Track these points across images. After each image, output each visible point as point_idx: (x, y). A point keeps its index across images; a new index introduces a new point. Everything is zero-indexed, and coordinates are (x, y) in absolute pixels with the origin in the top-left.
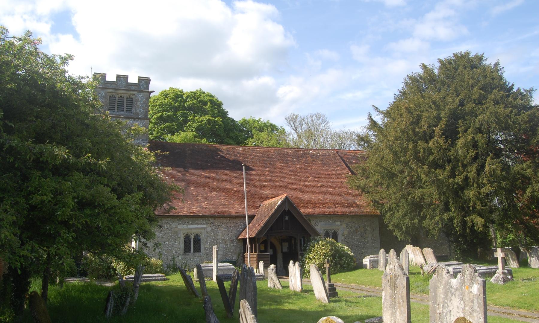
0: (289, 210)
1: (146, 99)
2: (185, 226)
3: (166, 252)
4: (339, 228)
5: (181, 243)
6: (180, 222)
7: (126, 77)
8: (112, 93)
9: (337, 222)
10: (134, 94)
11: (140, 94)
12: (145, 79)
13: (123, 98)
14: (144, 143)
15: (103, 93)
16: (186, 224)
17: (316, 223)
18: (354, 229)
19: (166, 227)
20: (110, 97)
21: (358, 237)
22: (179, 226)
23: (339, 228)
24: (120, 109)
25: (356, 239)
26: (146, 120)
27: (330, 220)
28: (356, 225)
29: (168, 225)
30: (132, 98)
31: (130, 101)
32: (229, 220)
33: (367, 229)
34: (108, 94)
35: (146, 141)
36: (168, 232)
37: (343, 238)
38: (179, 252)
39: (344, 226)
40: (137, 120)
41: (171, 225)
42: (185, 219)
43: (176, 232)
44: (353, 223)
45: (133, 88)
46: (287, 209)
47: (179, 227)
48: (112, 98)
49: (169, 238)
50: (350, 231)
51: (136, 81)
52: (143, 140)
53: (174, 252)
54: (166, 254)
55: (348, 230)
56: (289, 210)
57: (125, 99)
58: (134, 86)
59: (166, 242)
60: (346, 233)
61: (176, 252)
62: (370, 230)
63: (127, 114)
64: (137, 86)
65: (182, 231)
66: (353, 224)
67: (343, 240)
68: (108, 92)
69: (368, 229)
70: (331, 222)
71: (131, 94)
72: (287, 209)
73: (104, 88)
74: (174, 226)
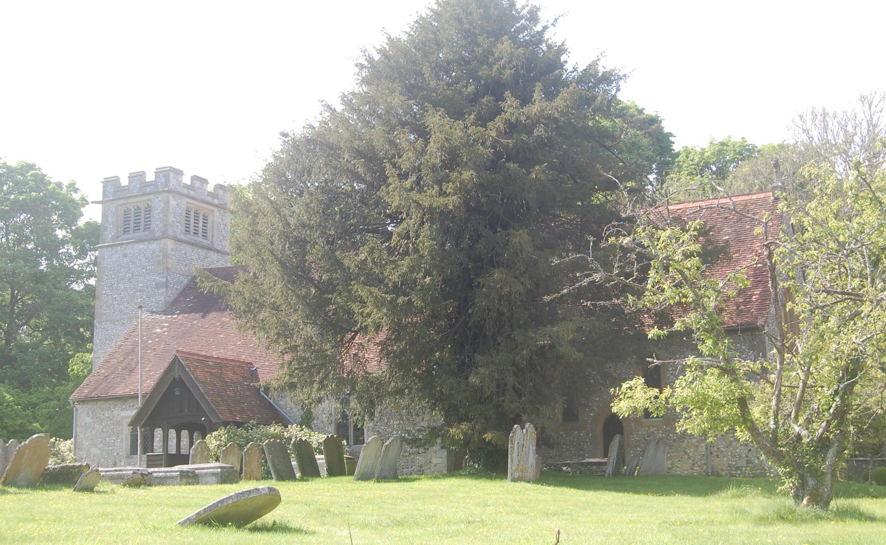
1: (165, 204)
2: (129, 412)
5: (124, 439)
6: (124, 407)
7: (141, 175)
8: (124, 204)
10: (151, 200)
11: (158, 198)
12: (163, 171)
13: (140, 209)
16: (131, 408)
19: (107, 415)
20: (125, 211)
26: (163, 240)
29: (110, 413)
31: (149, 210)
34: (120, 208)
35: (162, 275)
38: (121, 454)
40: (153, 241)
41: (113, 411)
42: (130, 401)
43: (119, 423)
45: (148, 190)
47: (122, 415)
48: (127, 213)
51: (153, 179)
52: (159, 274)
53: (115, 454)
57: (143, 211)
59: (107, 439)
61: (118, 454)
63: (143, 234)
64: (152, 185)
65: (125, 421)
71: (148, 200)
73: (112, 200)
74: (116, 414)
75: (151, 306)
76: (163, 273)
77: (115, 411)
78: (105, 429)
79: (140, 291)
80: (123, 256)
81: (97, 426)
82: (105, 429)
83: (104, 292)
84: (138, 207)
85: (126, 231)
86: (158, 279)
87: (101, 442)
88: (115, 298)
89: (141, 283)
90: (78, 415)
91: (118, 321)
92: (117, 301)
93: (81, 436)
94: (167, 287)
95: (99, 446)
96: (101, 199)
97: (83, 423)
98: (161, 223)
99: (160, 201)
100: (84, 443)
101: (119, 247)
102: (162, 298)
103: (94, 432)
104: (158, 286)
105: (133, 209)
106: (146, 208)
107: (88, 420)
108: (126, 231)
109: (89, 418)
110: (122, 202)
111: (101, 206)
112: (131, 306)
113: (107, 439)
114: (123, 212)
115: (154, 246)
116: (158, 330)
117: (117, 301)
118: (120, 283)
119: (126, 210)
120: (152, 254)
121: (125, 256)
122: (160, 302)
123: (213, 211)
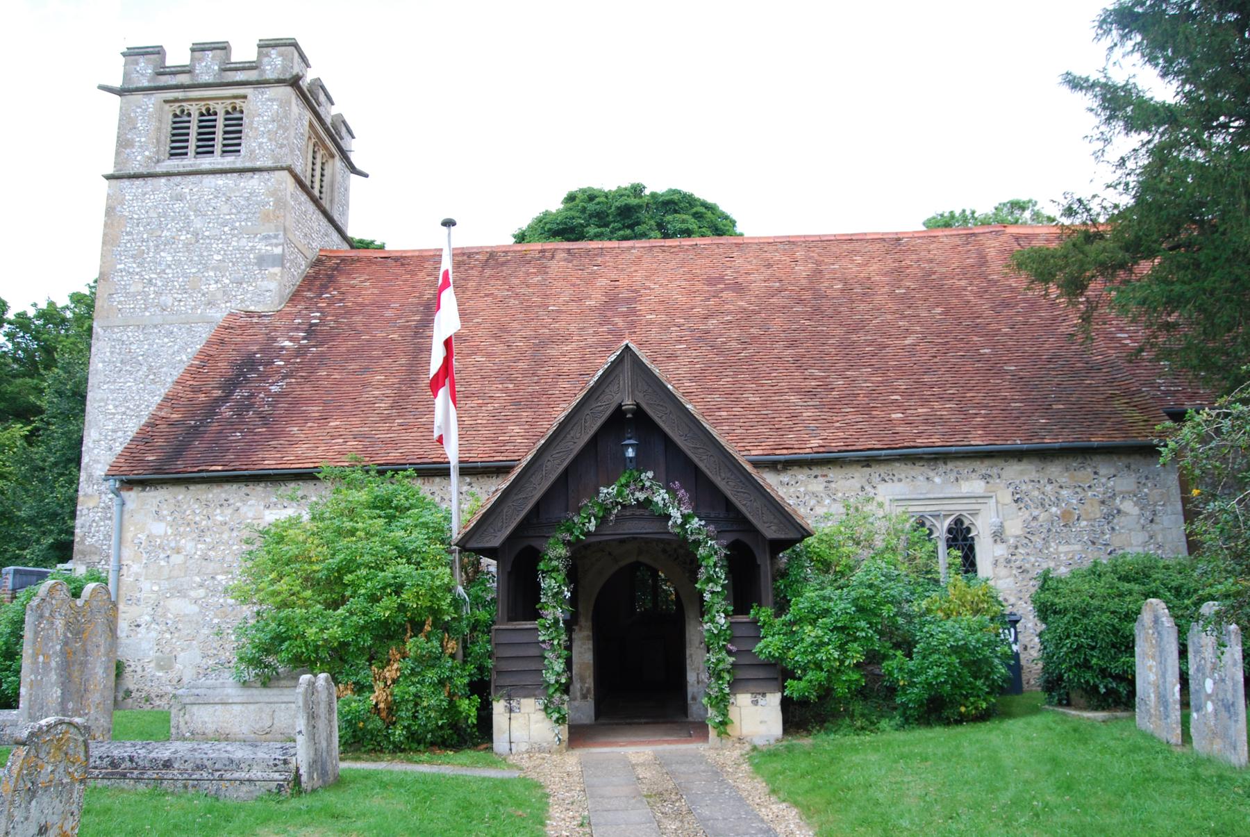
0: (638, 405)
3: (216, 616)
4: (977, 507)
8: (176, 100)
9: (967, 479)
10: (245, 97)
14: (269, 248)
15: (151, 102)
17: (863, 488)
18: (1054, 509)
19: (219, 518)
21: (1078, 547)
22: (267, 512)
23: (977, 507)
24: (205, 147)
25: (1066, 553)
27: (931, 474)
28: (1064, 492)
29: (229, 511)
30: (242, 112)
32: (470, 484)
33: (1119, 511)
35: (274, 241)
36: (225, 536)
37: (1001, 551)
39: (1006, 496)
40: (250, 174)
44: (1050, 481)
46: (628, 403)
49: (229, 558)
50: (1035, 518)
52: (267, 238)
54: (216, 621)
55: (1025, 514)
56: (639, 412)
58: (244, 69)
59: (219, 577)
60: (1014, 528)
62: (1135, 511)
63: (220, 160)
66: (1049, 488)
67: (1002, 560)
68: (166, 102)
69: (1129, 506)
70: (937, 480)
72: (628, 403)
74: (250, 515)
75: (242, 301)
76: (276, 237)
77: (244, 509)
78: (212, 553)
79: (215, 269)
80: (171, 197)
81: (188, 544)
82: (212, 553)
83: (122, 266)
84: (208, 110)
85: (177, 151)
86: (262, 247)
87: (201, 586)
88: (150, 280)
89: (219, 253)
90: (126, 517)
91: (155, 326)
92: (155, 285)
93: (136, 568)
94: (283, 266)
95: (193, 594)
96: (117, 83)
97: (142, 537)
98: (270, 140)
99: (269, 100)
100: (146, 585)
101: (163, 180)
102: (273, 285)
103: (177, 559)
104: (262, 261)
105: (197, 113)
106: (227, 113)
107: (159, 528)
108: (177, 151)
109: (163, 525)
110: (179, 94)
111: (117, 99)
112: (190, 296)
113: (219, 577)
114: (171, 116)
115: (254, 183)
116: (287, 343)
117: (155, 285)
118: (163, 251)
119: (178, 112)
120: (248, 199)
121: (180, 198)
122: (268, 294)
123: (332, 156)
